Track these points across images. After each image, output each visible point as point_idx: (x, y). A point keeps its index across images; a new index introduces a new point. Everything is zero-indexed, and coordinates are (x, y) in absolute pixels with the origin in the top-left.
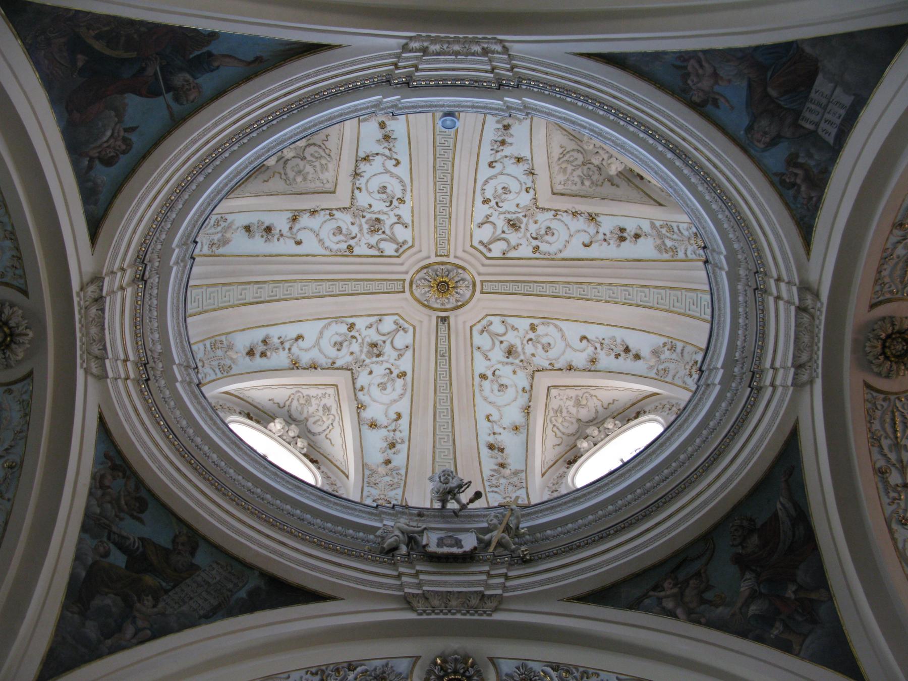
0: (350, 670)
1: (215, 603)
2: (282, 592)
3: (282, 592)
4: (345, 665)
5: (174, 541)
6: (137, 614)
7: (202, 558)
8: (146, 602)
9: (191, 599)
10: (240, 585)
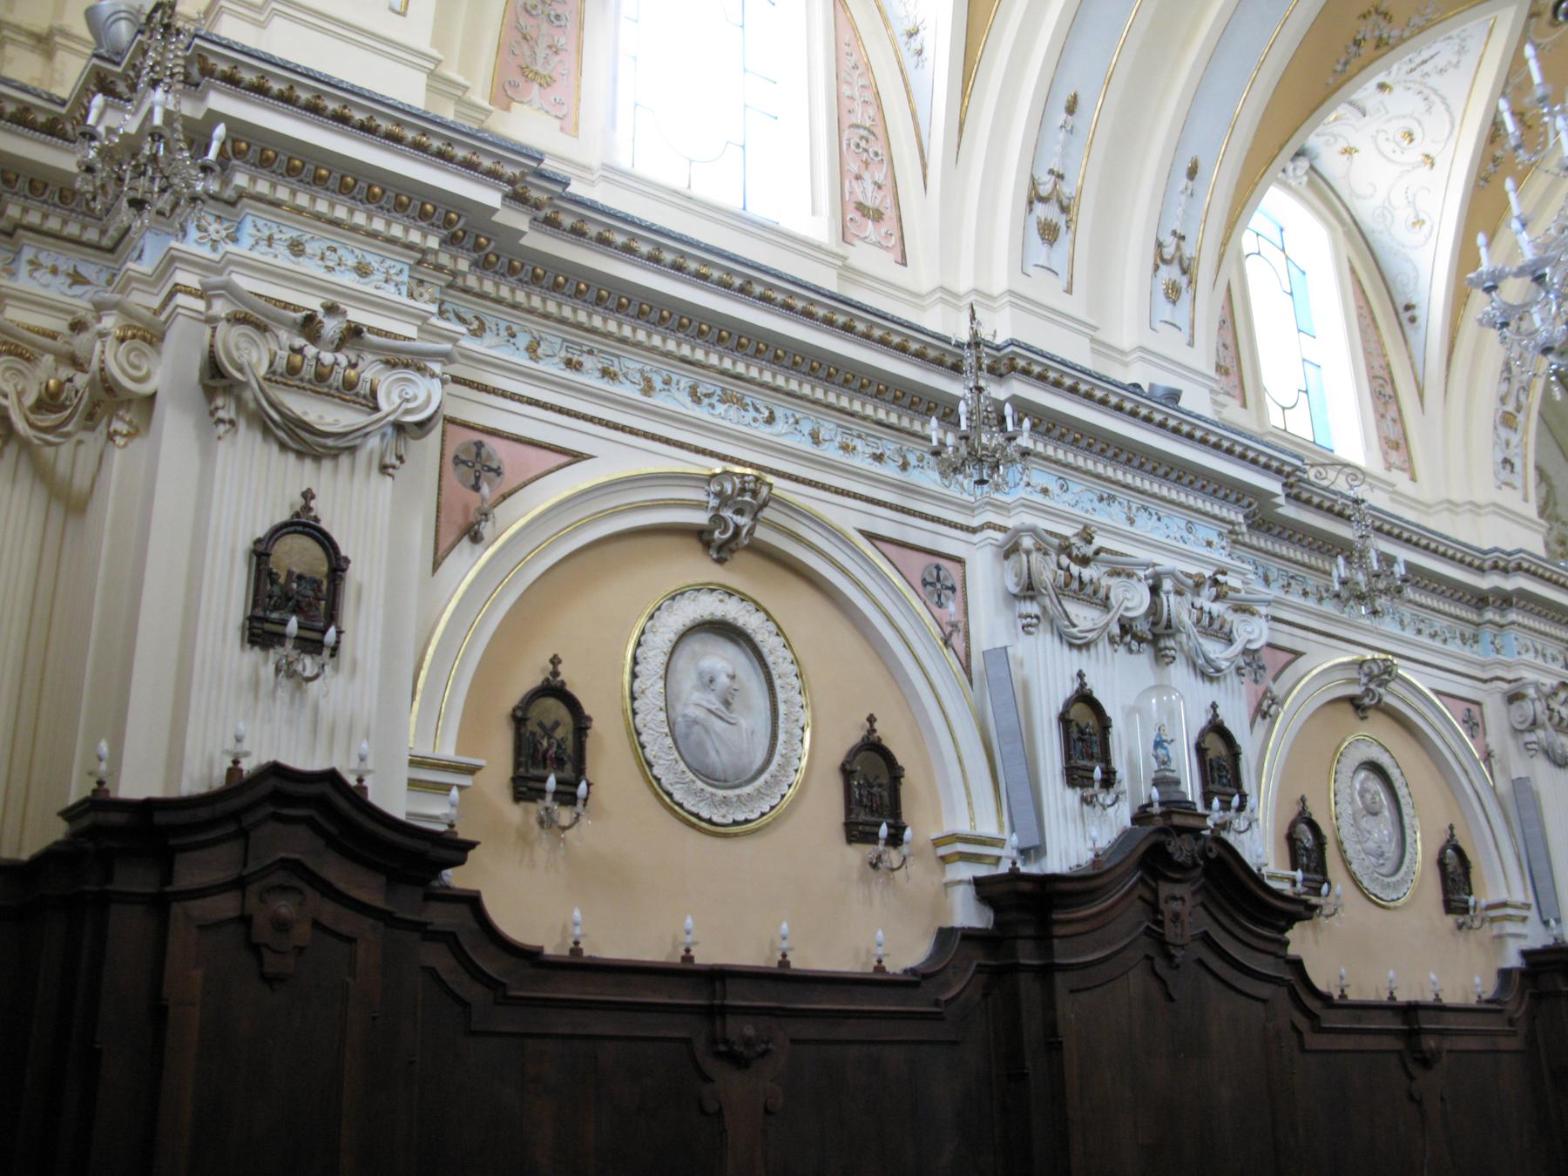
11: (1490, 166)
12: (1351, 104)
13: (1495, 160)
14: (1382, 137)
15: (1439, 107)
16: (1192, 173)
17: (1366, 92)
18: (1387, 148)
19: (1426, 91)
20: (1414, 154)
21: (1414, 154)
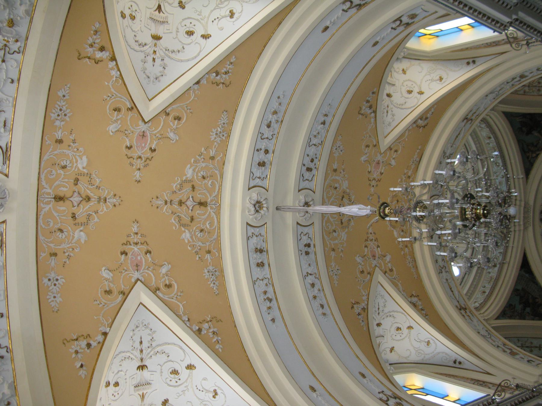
2: (525, 265)
3: (525, 265)
7: (520, 287)
11: (423, 312)
12: (377, 337)
13: (422, 310)
14: (394, 336)
15: (395, 314)
16: (363, 376)
17: (378, 331)
18: (398, 337)
19: (388, 314)
20: (405, 331)
21: (405, 331)
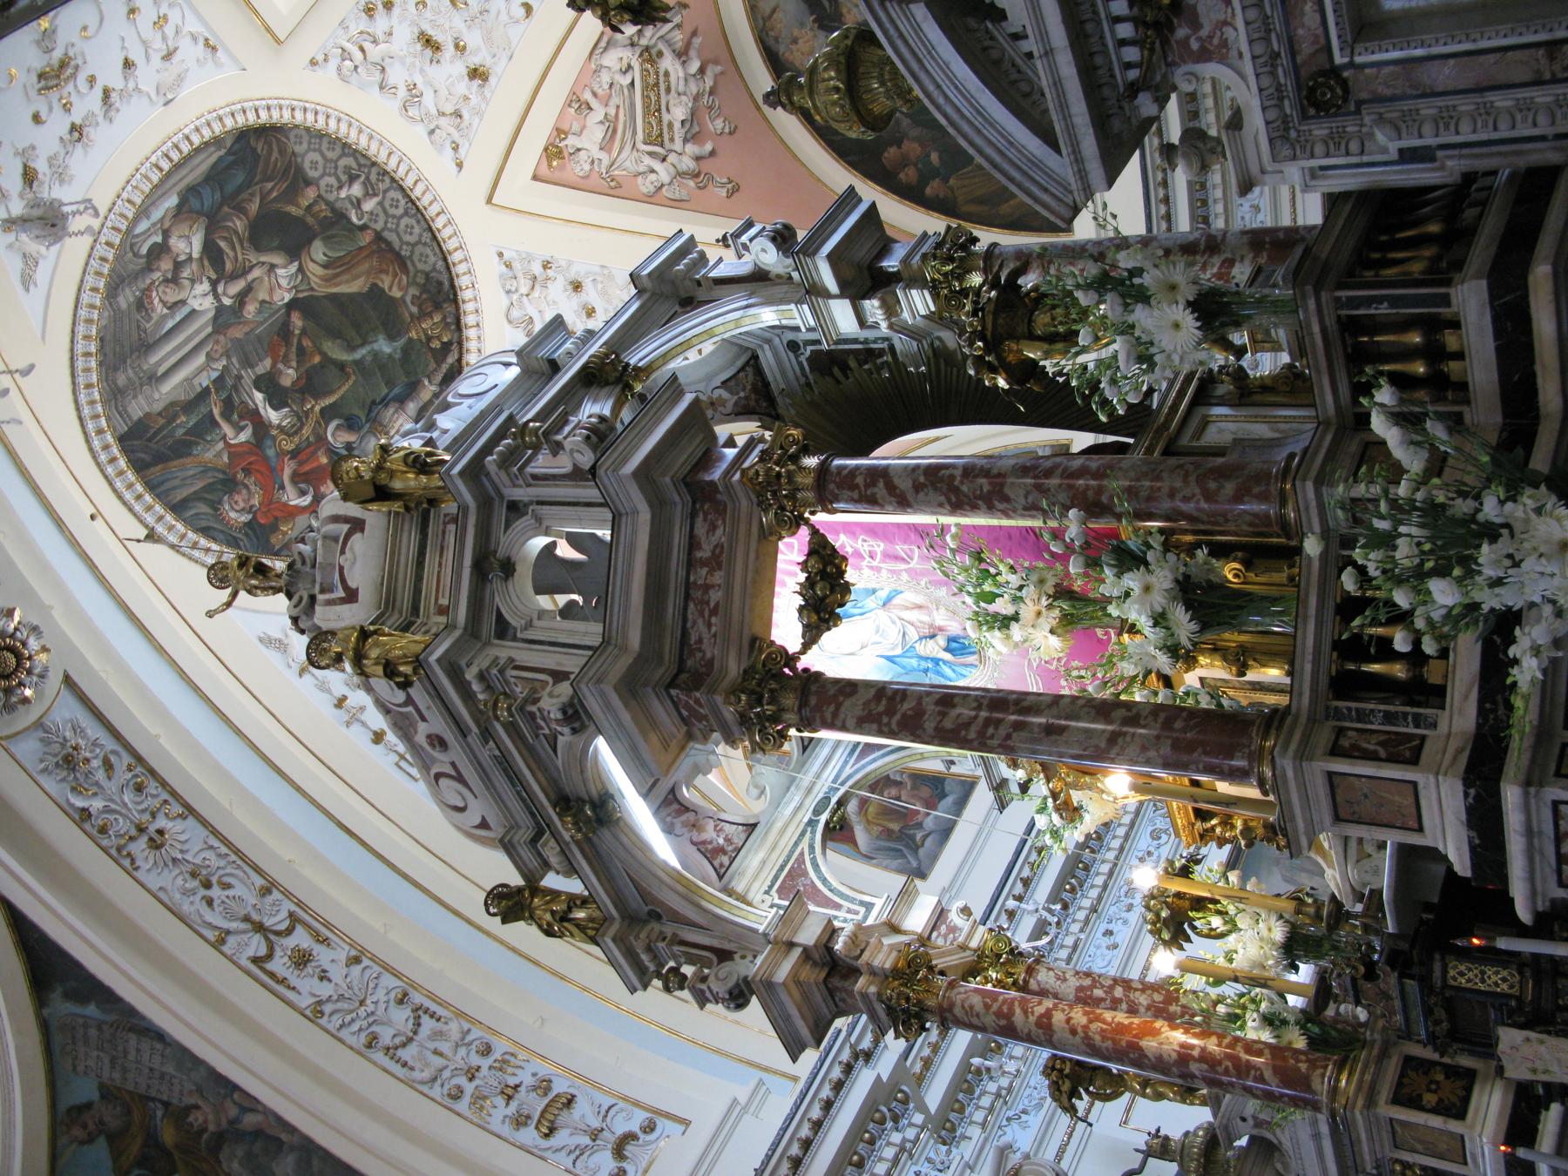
0: (90, 815)
1: (133, 1039)
4: (87, 826)
5: (91, 1140)
6: (224, 1123)
7: (84, 1090)
8: (201, 1120)
9: (151, 1069)
10: (81, 1021)
